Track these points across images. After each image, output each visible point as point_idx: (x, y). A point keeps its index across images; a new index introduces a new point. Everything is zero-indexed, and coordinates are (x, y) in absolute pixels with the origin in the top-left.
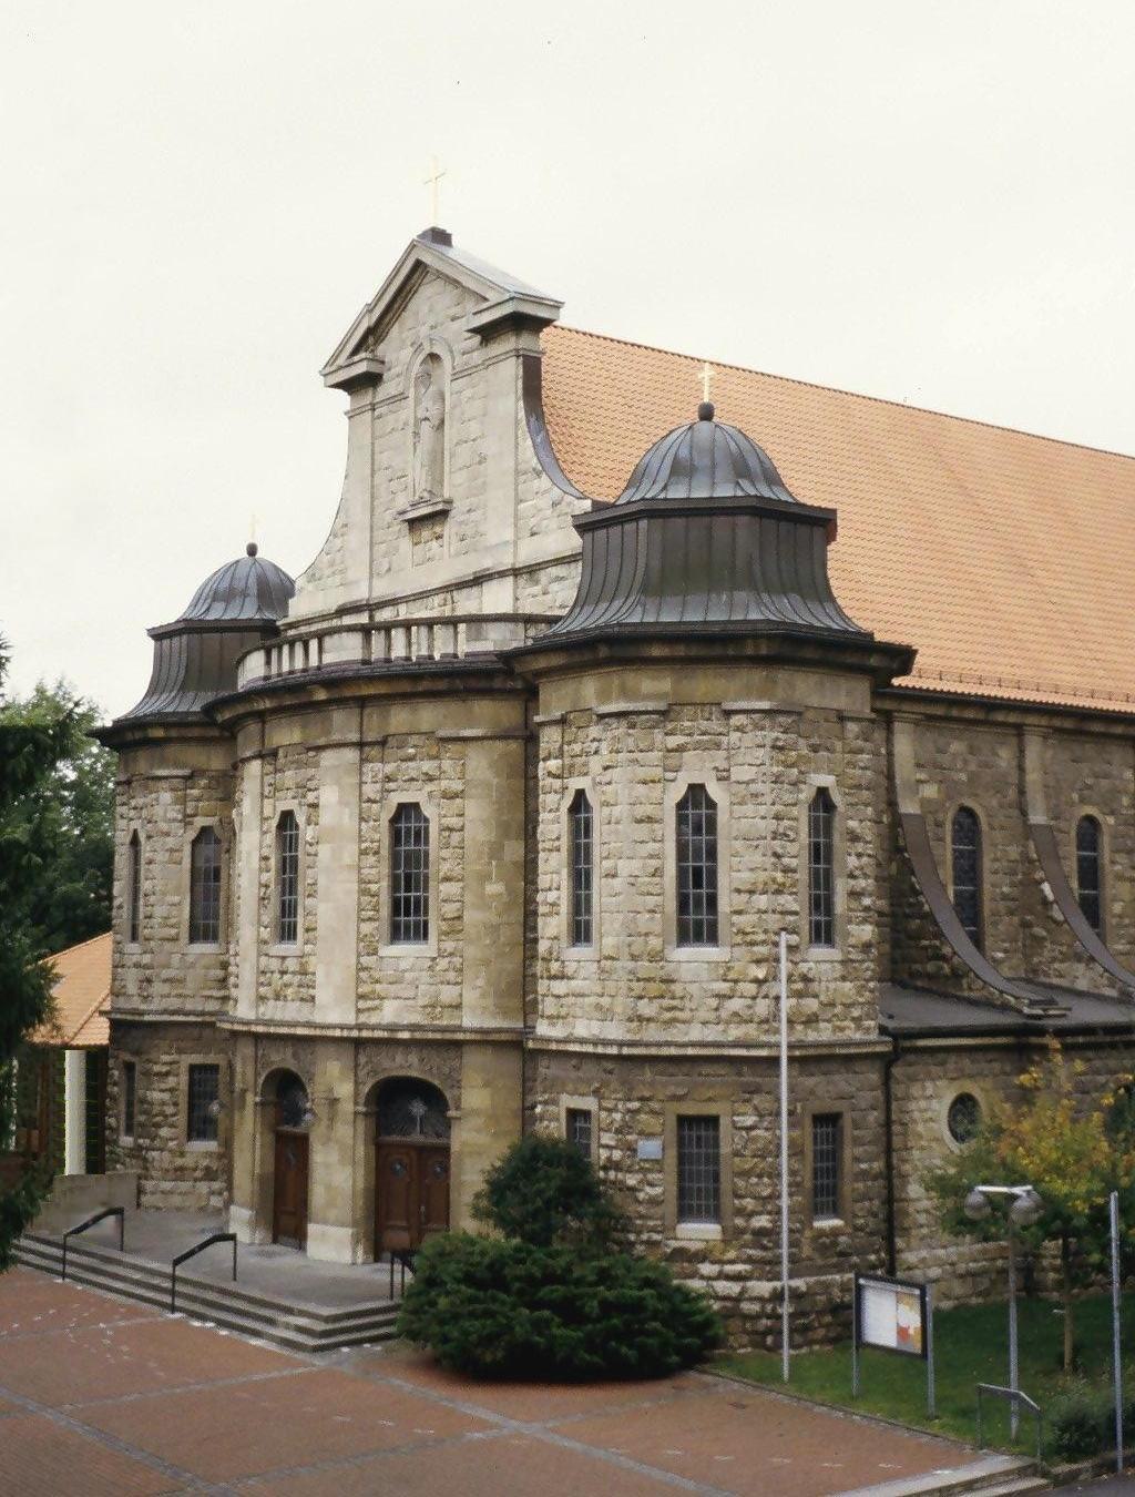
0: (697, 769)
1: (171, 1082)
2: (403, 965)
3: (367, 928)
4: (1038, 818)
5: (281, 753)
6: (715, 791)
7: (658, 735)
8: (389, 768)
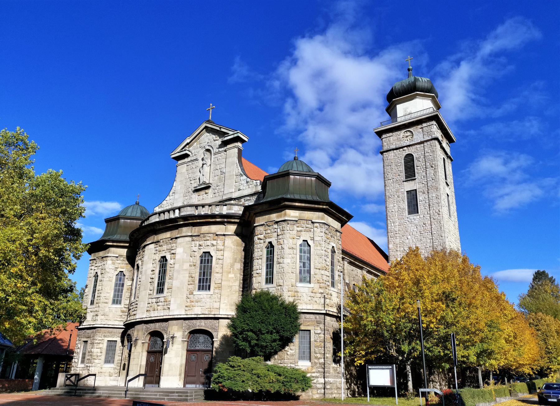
0: (306, 236)
1: (101, 346)
2: (202, 296)
3: (190, 287)
4: (347, 281)
5: (162, 241)
6: (310, 242)
7: (295, 226)
8: (201, 243)
